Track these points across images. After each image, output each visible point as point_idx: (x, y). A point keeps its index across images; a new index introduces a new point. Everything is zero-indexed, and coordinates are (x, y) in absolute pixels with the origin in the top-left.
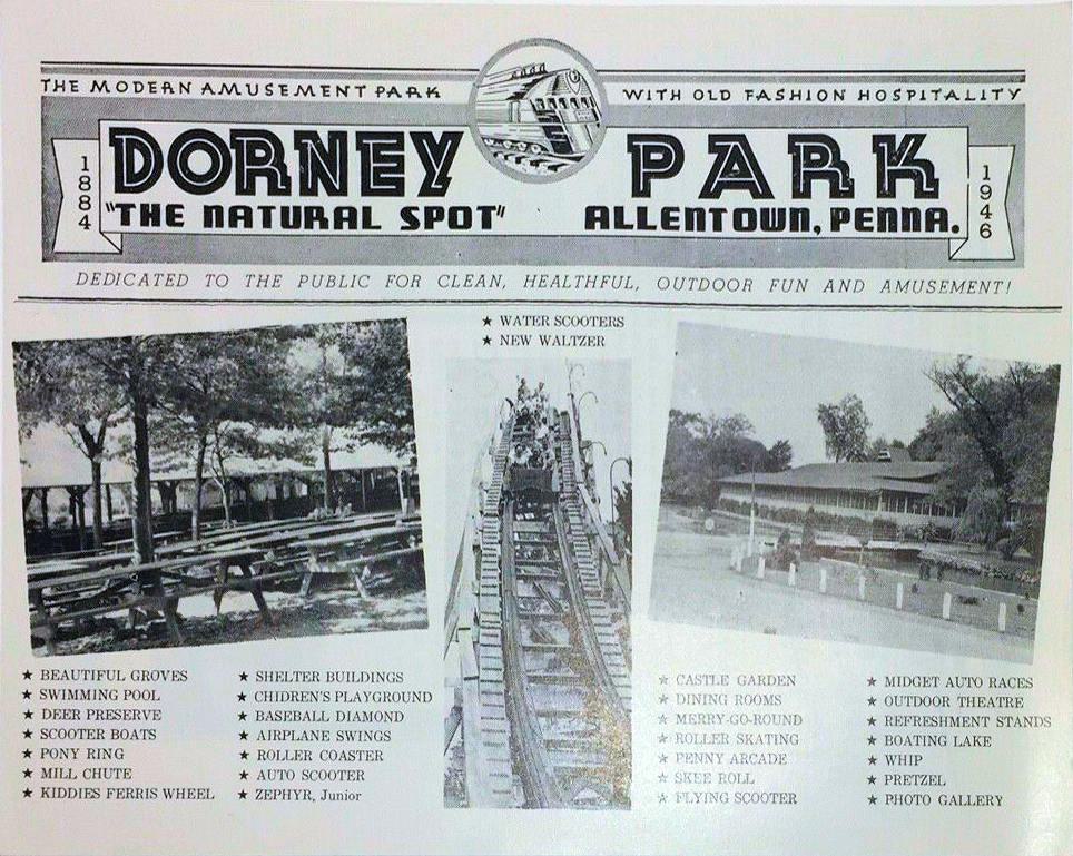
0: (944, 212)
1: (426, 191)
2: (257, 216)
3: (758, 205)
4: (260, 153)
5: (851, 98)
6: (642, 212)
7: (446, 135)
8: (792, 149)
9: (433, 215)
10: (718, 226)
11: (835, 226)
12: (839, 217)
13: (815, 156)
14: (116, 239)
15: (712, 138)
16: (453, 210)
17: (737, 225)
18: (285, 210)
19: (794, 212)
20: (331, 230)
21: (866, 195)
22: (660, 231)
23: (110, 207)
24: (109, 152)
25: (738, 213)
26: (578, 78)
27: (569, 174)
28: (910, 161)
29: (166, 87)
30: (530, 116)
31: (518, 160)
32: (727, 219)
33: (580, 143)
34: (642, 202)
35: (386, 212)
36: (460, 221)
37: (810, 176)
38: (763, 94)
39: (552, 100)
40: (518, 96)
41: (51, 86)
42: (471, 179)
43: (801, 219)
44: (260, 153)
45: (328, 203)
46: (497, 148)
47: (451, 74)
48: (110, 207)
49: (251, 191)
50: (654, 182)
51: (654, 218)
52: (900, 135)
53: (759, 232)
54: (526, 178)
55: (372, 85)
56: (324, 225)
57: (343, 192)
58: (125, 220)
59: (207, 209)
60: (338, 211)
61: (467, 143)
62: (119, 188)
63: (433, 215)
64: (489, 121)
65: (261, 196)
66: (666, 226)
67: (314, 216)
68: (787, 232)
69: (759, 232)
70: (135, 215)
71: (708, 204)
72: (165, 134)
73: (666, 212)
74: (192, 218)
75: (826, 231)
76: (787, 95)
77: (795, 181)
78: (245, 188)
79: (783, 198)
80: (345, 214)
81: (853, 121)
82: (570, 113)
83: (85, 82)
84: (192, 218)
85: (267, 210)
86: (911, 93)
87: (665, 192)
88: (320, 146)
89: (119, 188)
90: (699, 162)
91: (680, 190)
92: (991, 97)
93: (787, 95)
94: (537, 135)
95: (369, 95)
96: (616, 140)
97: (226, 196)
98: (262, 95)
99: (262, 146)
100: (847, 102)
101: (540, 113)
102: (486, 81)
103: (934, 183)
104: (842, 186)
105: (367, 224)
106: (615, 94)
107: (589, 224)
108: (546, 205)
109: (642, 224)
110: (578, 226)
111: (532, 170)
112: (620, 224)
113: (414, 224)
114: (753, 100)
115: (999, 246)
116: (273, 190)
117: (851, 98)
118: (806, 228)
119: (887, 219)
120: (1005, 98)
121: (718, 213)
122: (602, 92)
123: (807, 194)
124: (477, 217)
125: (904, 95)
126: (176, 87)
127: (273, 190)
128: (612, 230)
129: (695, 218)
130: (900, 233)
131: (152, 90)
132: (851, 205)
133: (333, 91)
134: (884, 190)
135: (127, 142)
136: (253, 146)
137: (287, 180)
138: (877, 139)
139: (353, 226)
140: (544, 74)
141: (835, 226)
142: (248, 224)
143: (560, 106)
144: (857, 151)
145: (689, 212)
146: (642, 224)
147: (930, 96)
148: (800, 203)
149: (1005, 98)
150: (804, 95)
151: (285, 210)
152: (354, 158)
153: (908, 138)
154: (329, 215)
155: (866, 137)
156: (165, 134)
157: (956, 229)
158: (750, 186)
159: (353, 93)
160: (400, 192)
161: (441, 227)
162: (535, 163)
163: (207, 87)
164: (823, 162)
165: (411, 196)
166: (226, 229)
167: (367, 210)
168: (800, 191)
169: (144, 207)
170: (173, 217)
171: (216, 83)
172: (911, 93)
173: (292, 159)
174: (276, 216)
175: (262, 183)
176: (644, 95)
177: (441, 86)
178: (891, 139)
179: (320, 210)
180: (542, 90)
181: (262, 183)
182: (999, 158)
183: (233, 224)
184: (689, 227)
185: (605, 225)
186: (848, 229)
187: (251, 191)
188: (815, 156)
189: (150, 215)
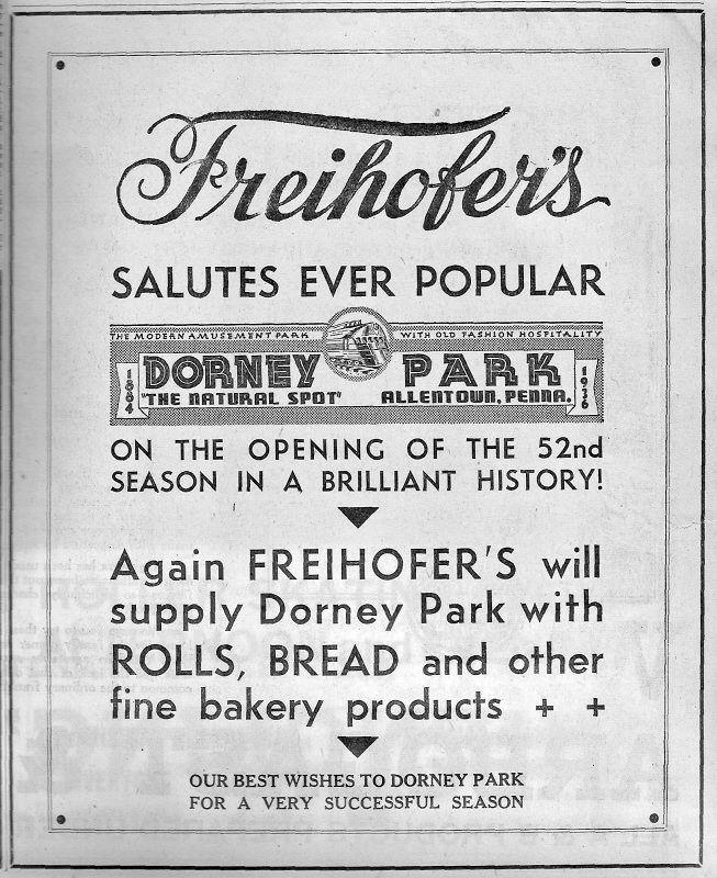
1: (300, 385)
2: (216, 398)
3: (469, 389)
4: (217, 367)
5: (516, 335)
6: (410, 394)
7: (311, 357)
9: (305, 396)
10: (449, 400)
11: (508, 400)
14: (146, 411)
15: (446, 356)
16: (315, 394)
17: (459, 399)
18: (230, 395)
19: (488, 392)
20: (253, 405)
21: (523, 384)
22: (420, 403)
23: (144, 396)
28: (545, 366)
29: (172, 336)
30: (354, 347)
31: (348, 369)
32: (453, 397)
33: (380, 359)
34: (411, 389)
35: (281, 396)
36: (319, 400)
37: (495, 375)
38: (471, 334)
39: (365, 339)
40: (346, 337)
41: (116, 337)
42: (324, 378)
43: (491, 396)
45: (252, 392)
46: (339, 364)
47: (315, 326)
48: (144, 396)
49: (213, 386)
50: (416, 379)
51: (416, 397)
52: (540, 353)
53: (470, 403)
54: (352, 378)
55: (274, 334)
56: (250, 403)
57: (260, 385)
58: (151, 403)
59: (191, 395)
60: (257, 395)
61: (322, 359)
62: (148, 387)
63: (305, 396)
64: (335, 348)
65: (219, 388)
66: (422, 400)
67: (245, 397)
68: (483, 403)
69: (470, 403)
70: (156, 399)
71: (443, 389)
72: (171, 359)
74: (184, 401)
75: (504, 402)
76: (484, 334)
79: (482, 386)
80: (260, 397)
81: (518, 345)
83: (132, 336)
84: (184, 401)
85: (221, 395)
87: (422, 383)
89: (148, 387)
91: (429, 383)
92: (586, 335)
93: (484, 334)
94: (356, 355)
95: (273, 336)
96: (397, 358)
97: (201, 389)
98: (218, 338)
99: (219, 364)
103: (558, 378)
104: (512, 379)
106: (397, 335)
107: (384, 401)
108: (363, 392)
109: (411, 399)
110: (379, 402)
111: (354, 374)
112: (399, 400)
113: (295, 401)
115: (592, 410)
116: (224, 386)
117: (516, 335)
118: (493, 400)
119: (534, 396)
120: (593, 335)
121: (449, 393)
122: (391, 335)
123: (494, 384)
124: (327, 398)
126: (176, 336)
127: (224, 386)
128: (395, 403)
129: (437, 396)
130: (541, 403)
133: (254, 336)
134: (533, 381)
135: (152, 363)
137: (231, 380)
138: (529, 356)
139: (264, 403)
140: (361, 326)
141: (508, 400)
143: (369, 342)
144: (519, 360)
145: (434, 393)
146: (411, 399)
147: (556, 336)
151: (230, 395)
152: (265, 368)
154: (252, 397)
155: (523, 355)
156: (171, 359)
157: (569, 400)
159: (264, 337)
161: (309, 403)
162: (356, 370)
163: (192, 336)
164: (502, 368)
165: (294, 388)
166: (201, 406)
167: (271, 395)
168: (491, 381)
169: (160, 395)
170: (174, 398)
171: (196, 334)
173: (233, 370)
174: (226, 398)
175: (219, 382)
176: (411, 336)
177: (309, 333)
178: (536, 356)
180: (360, 334)
181: (219, 382)
182: (591, 365)
183: (204, 403)
184: (434, 401)
185: (392, 401)
186: (515, 401)
187: (213, 386)
189: (163, 399)
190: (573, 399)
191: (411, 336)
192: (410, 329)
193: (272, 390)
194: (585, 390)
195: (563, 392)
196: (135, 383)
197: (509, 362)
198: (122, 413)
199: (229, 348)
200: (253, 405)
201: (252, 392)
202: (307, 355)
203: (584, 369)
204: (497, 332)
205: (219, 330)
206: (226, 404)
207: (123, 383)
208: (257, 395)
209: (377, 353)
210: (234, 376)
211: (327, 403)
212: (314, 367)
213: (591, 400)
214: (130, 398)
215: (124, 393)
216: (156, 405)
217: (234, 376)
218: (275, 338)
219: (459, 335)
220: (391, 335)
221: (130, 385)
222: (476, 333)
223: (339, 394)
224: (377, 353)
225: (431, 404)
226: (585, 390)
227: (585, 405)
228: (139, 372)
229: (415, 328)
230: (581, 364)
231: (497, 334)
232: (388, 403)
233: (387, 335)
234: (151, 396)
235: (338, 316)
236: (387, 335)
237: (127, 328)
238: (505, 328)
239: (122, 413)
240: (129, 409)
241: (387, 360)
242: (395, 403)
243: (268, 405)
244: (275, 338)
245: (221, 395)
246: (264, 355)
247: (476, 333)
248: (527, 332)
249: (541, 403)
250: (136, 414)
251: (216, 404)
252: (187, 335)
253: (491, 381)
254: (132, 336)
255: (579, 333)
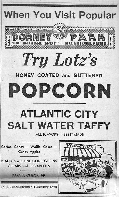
0: (106, 42)
2: (29, 43)
3: (85, 41)
6: (72, 42)
8: (89, 35)
9: (48, 43)
10: (80, 44)
12: (94, 43)
13: (91, 36)
14: (13, 46)
16: (51, 42)
17: (83, 44)
21: (97, 40)
22: (74, 45)
24: (12, 36)
25: (83, 42)
26: (65, 28)
27: (64, 38)
30: (59, 32)
32: (81, 43)
33: (65, 35)
34: (72, 41)
35: (43, 43)
37: (91, 38)
38: (85, 29)
40: (58, 30)
41: (6, 29)
42: (53, 39)
43: (90, 43)
44: (29, 36)
45: (36, 42)
46: (56, 36)
47: (51, 27)
51: (73, 43)
52: (101, 34)
53: (85, 45)
54: (60, 39)
58: (14, 44)
60: (38, 42)
61: (52, 34)
63: (48, 43)
65: (29, 41)
68: (88, 45)
71: (79, 41)
72: (18, 34)
73: (75, 43)
74: (21, 44)
75: (93, 45)
76: (88, 29)
77: (89, 39)
78: (27, 40)
79: (88, 41)
80: (38, 43)
82: (64, 31)
83: (10, 29)
84: (21, 44)
85: (30, 42)
86: (102, 29)
88: (35, 35)
90: (78, 36)
91: (76, 40)
92: (111, 30)
93: (88, 29)
96: (69, 34)
97: (25, 41)
98: (29, 30)
99: (30, 36)
100: (95, 30)
101: (60, 31)
102: (54, 28)
104: (94, 39)
105: (41, 44)
106: (69, 29)
107: (66, 44)
108: (61, 42)
109: (72, 43)
111: (59, 38)
112: (69, 44)
113: (46, 44)
114: (84, 30)
116: (30, 40)
117: (95, 29)
120: (113, 30)
121: (80, 42)
122: (68, 29)
124: (53, 43)
125: (101, 29)
127: (30, 40)
129: (78, 43)
131: (17, 29)
132: (95, 42)
134: (99, 40)
136: (28, 35)
138: (98, 34)
142: (27, 44)
144: (96, 35)
146: (72, 43)
147: (104, 30)
148: (90, 41)
149: (113, 30)
150: (90, 29)
152: (39, 37)
153: (102, 34)
154: (37, 43)
155: (97, 34)
156: (18, 34)
158: (84, 40)
159: (39, 29)
160: (45, 40)
161: (49, 44)
162: (60, 37)
165: (46, 41)
167: (41, 42)
168: (90, 40)
171: (24, 29)
172: (102, 29)
173: (32, 37)
174: (31, 43)
176: (72, 29)
179: (36, 42)
180: (61, 29)
182: (112, 36)
185: (68, 44)
186: (95, 44)
188: (91, 36)
189: (17, 43)
190: (108, 44)
191: (72, 29)
192: (72, 28)
193: (41, 41)
194: (111, 42)
195: (106, 42)
196: (10, 40)
197: (94, 36)
198: (7, 46)
199: (32, 32)
200: (37, 45)
201: (36, 42)
202: (49, 34)
203: (111, 37)
204: (91, 29)
205: (29, 28)
206: (31, 44)
207: (8, 39)
208: (38, 42)
209: (64, 33)
210: (33, 38)
211: (53, 44)
212: (50, 36)
213: (112, 44)
214: (9, 43)
215: (8, 42)
216: (15, 44)
217: (33, 38)
218: (42, 30)
219: (83, 29)
220: (68, 29)
221: (9, 40)
222: (86, 29)
223: (56, 42)
224: (64, 33)
225: (76, 45)
226: (111, 42)
227: (111, 45)
228: (11, 37)
229: (73, 28)
230: (110, 36)
231: (91, 30)
232: (67, 45)
233: (67, 29)
234: (14, 42)
235: (56, 25)
236: (67, 29)
237: (9, 27)
238: (93, 28)
239: (7, 46)
240: (9, 45)
241: (67, 35)
242: (68, 45)
243: (40, 45)
244: (42, 30)
245: (30, 42)
246: (39, 34)
247: (86, 29)
248: (98, 29)
249: (101, 45)
250: (11, 46)
251: (28, 44)
252: (22, 29)
253: (90, 40)
254: (10, 29)
255: (109, 29)
